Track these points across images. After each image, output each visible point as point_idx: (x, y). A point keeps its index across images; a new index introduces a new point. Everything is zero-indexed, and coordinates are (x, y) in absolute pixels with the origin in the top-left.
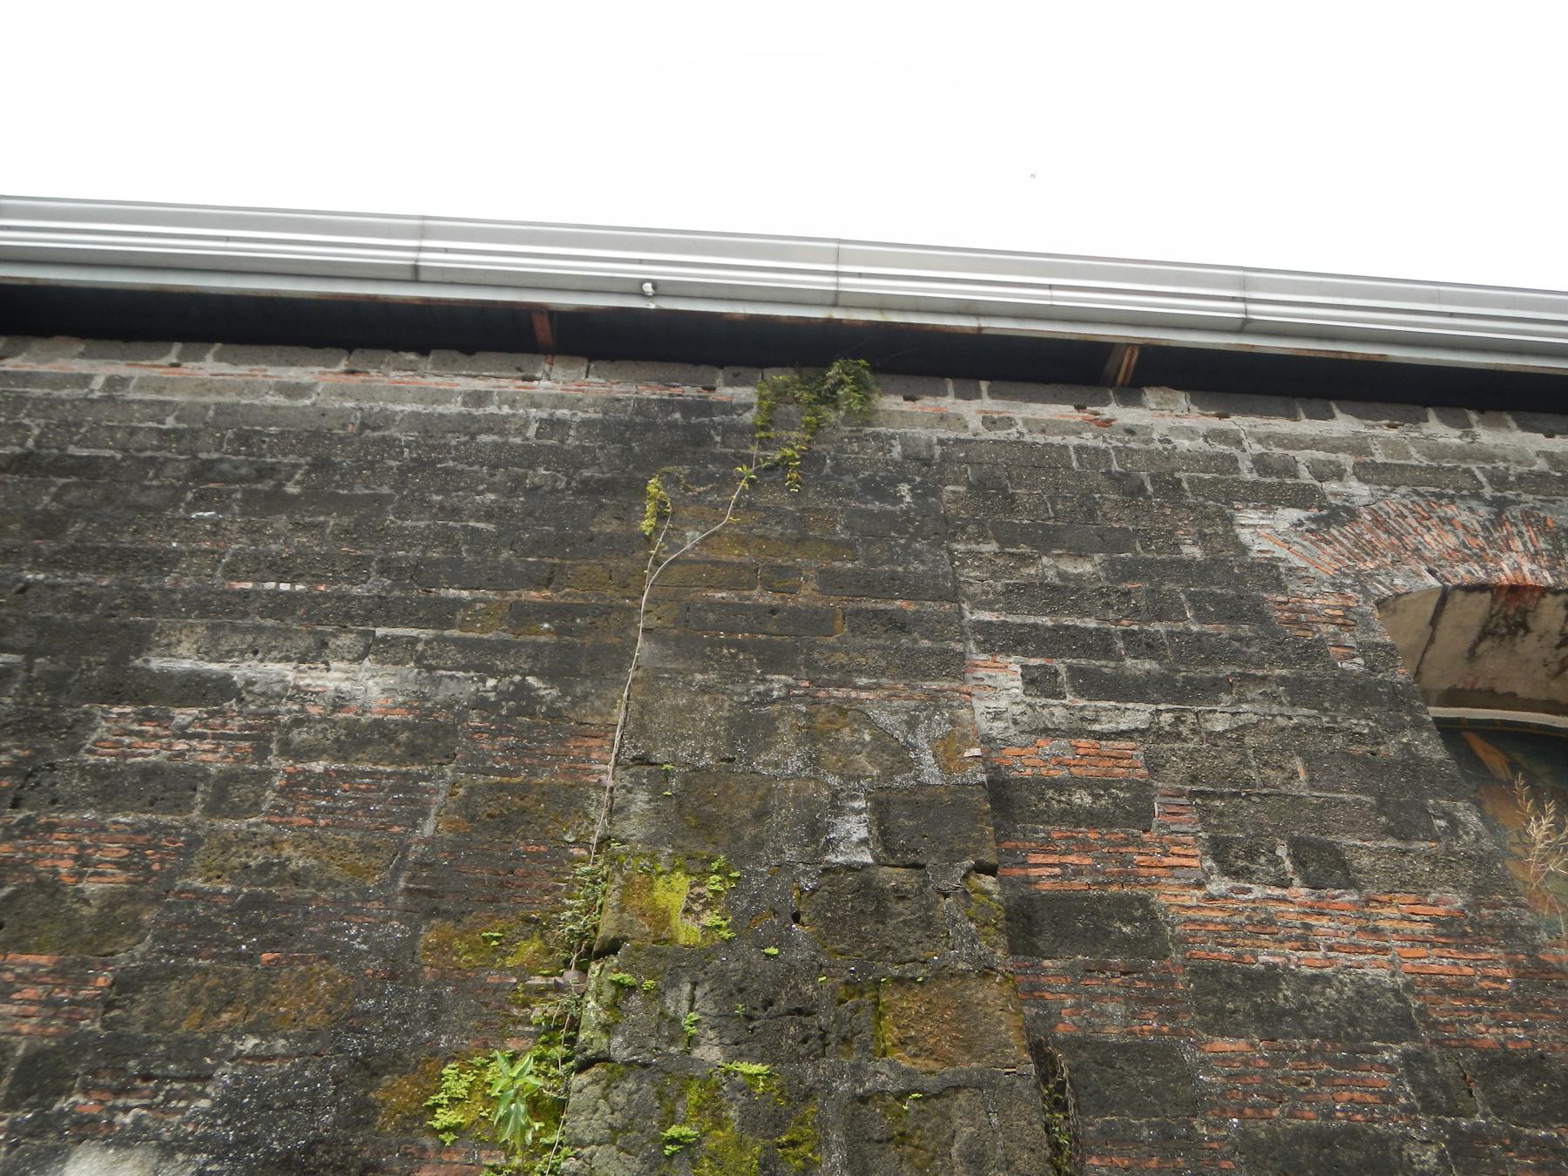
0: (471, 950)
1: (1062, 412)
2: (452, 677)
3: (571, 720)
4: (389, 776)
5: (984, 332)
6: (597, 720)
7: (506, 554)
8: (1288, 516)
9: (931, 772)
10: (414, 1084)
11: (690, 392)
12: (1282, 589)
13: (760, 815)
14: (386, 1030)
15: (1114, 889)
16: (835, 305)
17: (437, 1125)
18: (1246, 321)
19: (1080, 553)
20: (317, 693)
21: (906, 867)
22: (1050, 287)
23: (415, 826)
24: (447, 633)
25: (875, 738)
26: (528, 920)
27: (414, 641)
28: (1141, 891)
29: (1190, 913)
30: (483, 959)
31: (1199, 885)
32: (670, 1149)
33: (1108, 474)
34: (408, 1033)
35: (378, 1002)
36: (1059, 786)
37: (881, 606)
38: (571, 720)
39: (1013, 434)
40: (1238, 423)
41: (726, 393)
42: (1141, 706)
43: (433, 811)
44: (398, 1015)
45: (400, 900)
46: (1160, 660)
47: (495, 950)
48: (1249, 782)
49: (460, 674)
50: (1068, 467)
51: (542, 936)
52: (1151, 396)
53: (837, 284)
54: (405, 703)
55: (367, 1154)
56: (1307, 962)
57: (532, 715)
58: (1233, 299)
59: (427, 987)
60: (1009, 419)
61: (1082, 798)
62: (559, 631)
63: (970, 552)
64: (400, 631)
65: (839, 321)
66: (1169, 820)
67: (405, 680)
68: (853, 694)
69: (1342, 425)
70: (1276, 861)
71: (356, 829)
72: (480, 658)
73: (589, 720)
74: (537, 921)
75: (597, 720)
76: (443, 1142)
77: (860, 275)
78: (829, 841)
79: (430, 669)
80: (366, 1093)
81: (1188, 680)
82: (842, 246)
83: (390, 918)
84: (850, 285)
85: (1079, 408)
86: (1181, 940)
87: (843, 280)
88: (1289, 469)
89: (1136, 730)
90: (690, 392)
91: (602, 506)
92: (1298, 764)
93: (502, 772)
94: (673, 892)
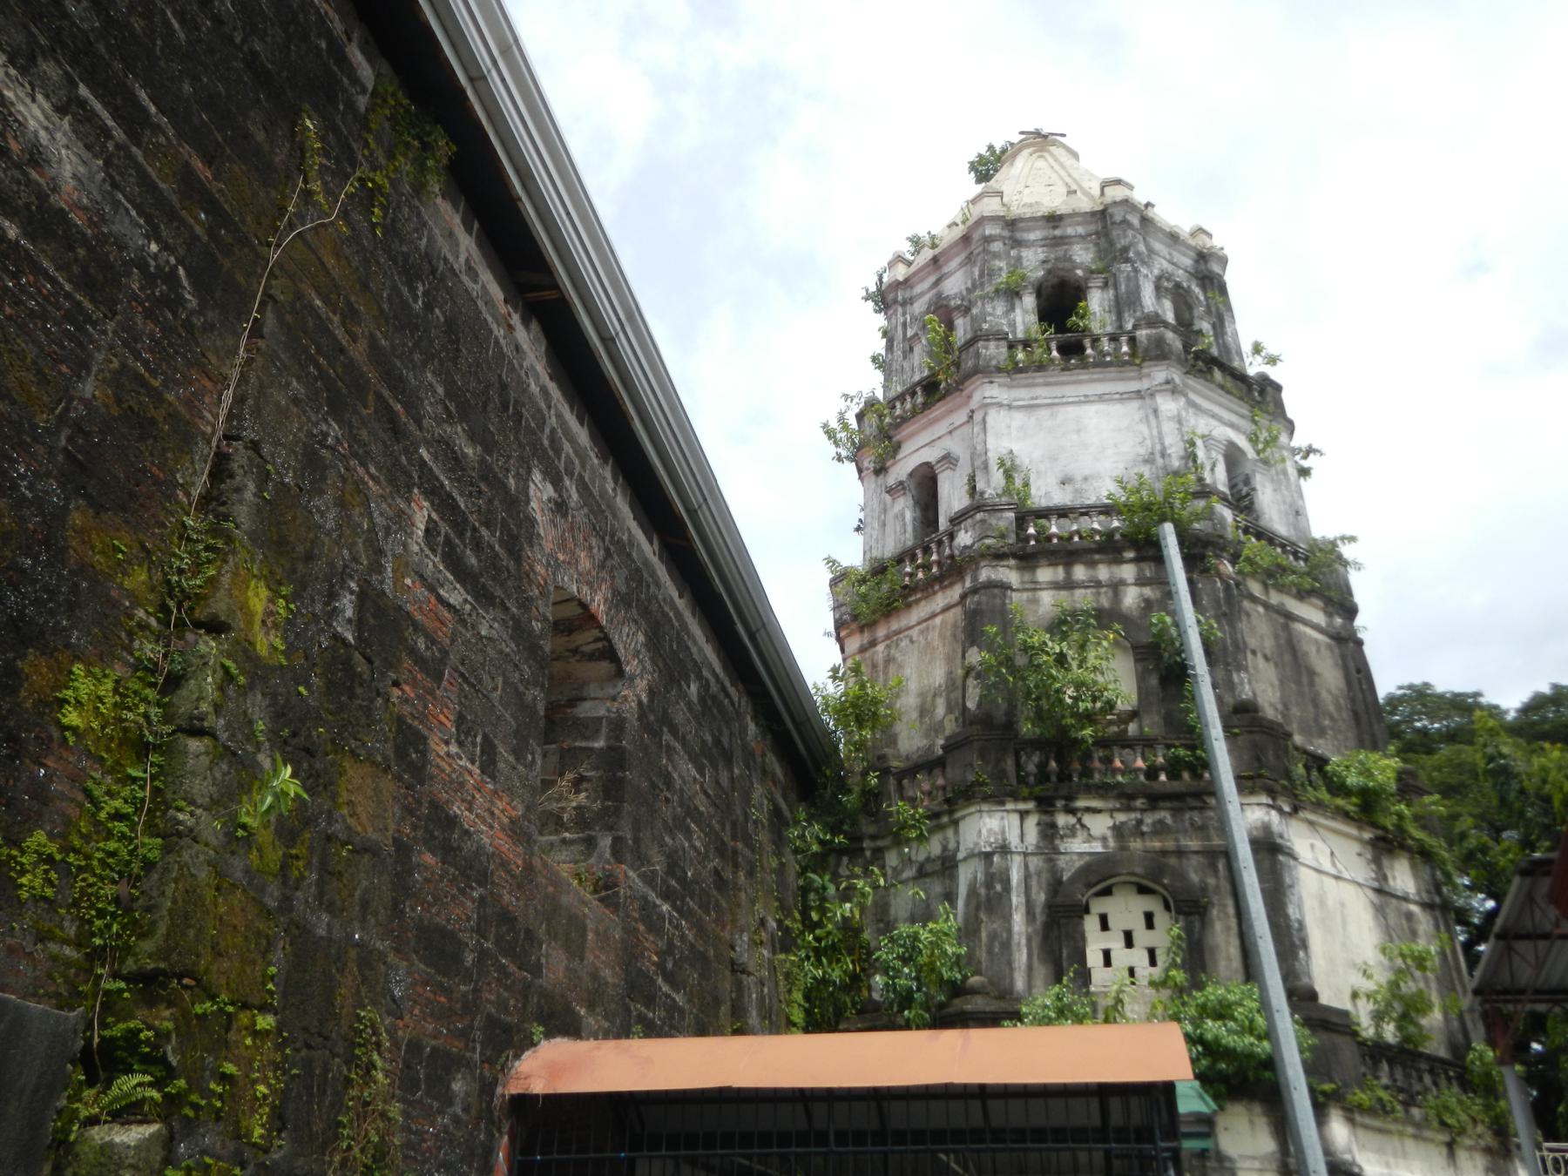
0: (103, 553)
1: (497, 293)
2: (127, 210)
3: (198, 345)
4: (68, 296)
5: (520, 205)
6: (214, 360)
7: (187, 88)
8: (549, 491)
9: (388, 587)
10: (50, 668)
11: (338, 26)
12: (532, 546)
13: (309, 558)
14: (36, 599)
15: (416, 723)
16: (471, 80)
17: (65, 721)
18: (613, 340)
19: (472, 438)
20: (16, 120)
21: (365, 657)
22: (568, 214)
23: (79, 377)
24: (134, 149)
25: (369, 530)
26: (144, 547)
27: (106, 133)
28: (426, 733)
29: (438, 760)
30: (109, 567)
31: (447, 743)
32: (240, 833)
33: (500, 376)
34: (51, 613)
35: (34, 566)
36: (417, 627)
37: (391, 401)
38: (198, 345)
39: (475, 289)
40: (553, 388)
41: (356, 56)
42: (462, 590)
43: (95, 369)
44: (45, 589)
45: (60, 458)
46: (480, 561)
47: (119, 563)
48: (480, 681)
49: (133, 213)
50: (487, 353)
51: (149, 570)
52: (535, 326)
53: (489, 71)
54: (85, 209)
55: (12, 723)
56: (467, 818)
57: (175, 314)
58: (619, 320)
59: (70, 572)
60: (477, 275)
61: (421, 644)
62: (211, 232)
63: (430, 385)
64: (98, 106)
65: (467, 99)
66: (449, 687)
67: (91, 178)
68: (366, 478)
69: (583, 435)
70: (474, 744)
71: (33, 342)
72: (157, 213)
73: (210, 355)
74: (148, 553)
75: (214, 360)
76: (65, 739)
77: (503, 80)
78: (335, 608)
79: (115, 185)
80: (15, 659)
81: (484, 586)
82: (514, 48)
83: (48, 475)
84: (494, 79)
85: (506, 301)
86: (432, 778)
87: (494, 73)
88: (558, 451)
89: (454, 607)
90: (338, 26)
91: (258, 100)
92: (500, 680)
93: (146, 363)
94: (258, 598)
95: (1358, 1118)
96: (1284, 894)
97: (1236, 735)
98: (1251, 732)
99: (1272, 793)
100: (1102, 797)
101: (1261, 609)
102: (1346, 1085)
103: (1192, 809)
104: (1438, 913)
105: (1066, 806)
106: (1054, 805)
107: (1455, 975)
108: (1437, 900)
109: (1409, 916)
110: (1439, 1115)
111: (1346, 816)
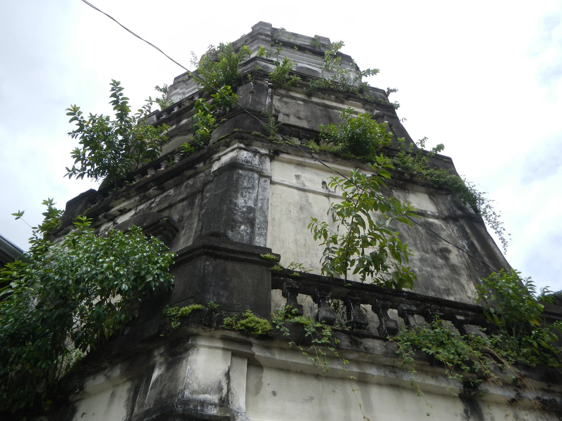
95: (258, 352)
96: (236, 192)
97: (224, 122)
98: (235, 116)
99: (241, 139)
100: (128, 198)
101: (301, 103)
102: (229, 309)
103: (189, 178)
104: (462, 222)
105: (105, 217)
106: (99, 220)
107: (486, 260)
108: (459, 212)
109: (428, 227)
110: (416, 347)
111: (337, 156)
